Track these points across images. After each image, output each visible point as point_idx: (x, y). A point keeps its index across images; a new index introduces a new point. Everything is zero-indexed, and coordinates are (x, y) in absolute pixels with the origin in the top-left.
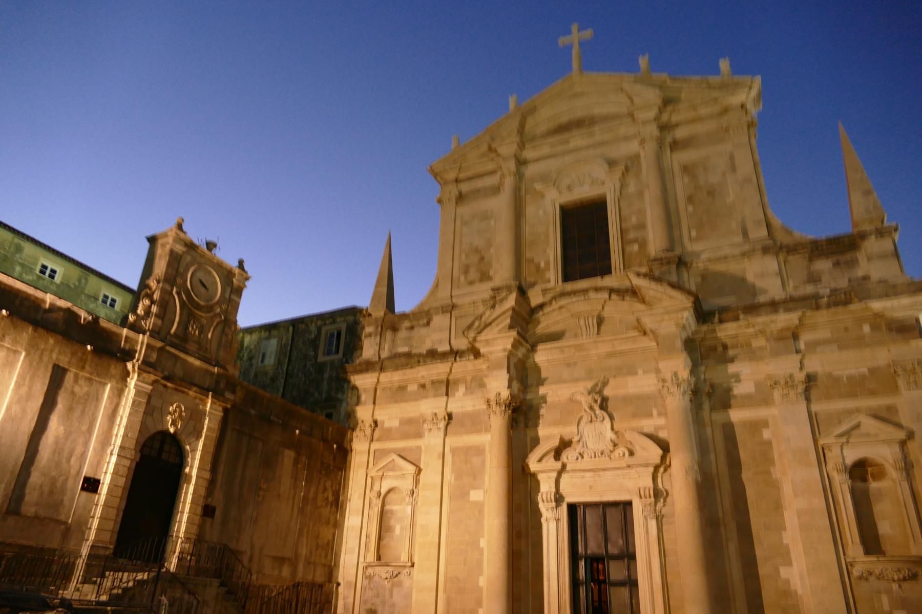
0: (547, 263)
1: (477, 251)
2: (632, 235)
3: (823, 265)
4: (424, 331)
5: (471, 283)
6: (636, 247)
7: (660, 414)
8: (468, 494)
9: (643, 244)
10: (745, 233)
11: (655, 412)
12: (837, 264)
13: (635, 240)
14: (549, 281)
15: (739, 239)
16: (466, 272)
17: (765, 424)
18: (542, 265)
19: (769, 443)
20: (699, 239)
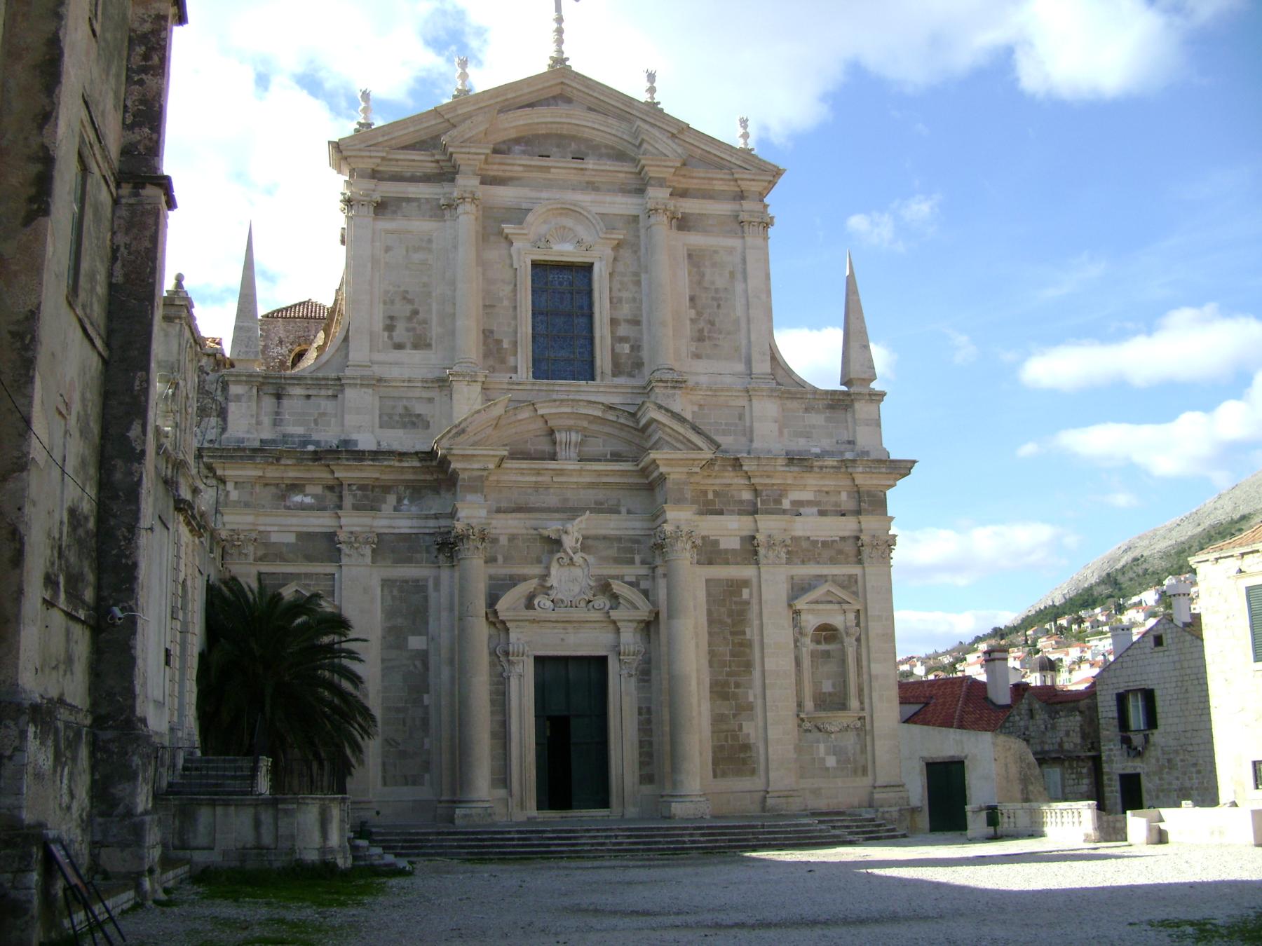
0: (515, 344)
1: (406, 299)
2: (623, 330)
3: (817, 419)
4: (327, 406)
5: (399, 346)
6: (626, 348)
7: (643, 562)
8: (406, 640)
9: (636, 348)
10: (749, 362)
11: (637, 558)
12: (828, 420)
13: (623, 340)
14: (515, 370)
15: (740, 367)
16: (390, 328)
17: (746, 583)
18: (505, 345)
19: (748, 603)
20: (697, 356)
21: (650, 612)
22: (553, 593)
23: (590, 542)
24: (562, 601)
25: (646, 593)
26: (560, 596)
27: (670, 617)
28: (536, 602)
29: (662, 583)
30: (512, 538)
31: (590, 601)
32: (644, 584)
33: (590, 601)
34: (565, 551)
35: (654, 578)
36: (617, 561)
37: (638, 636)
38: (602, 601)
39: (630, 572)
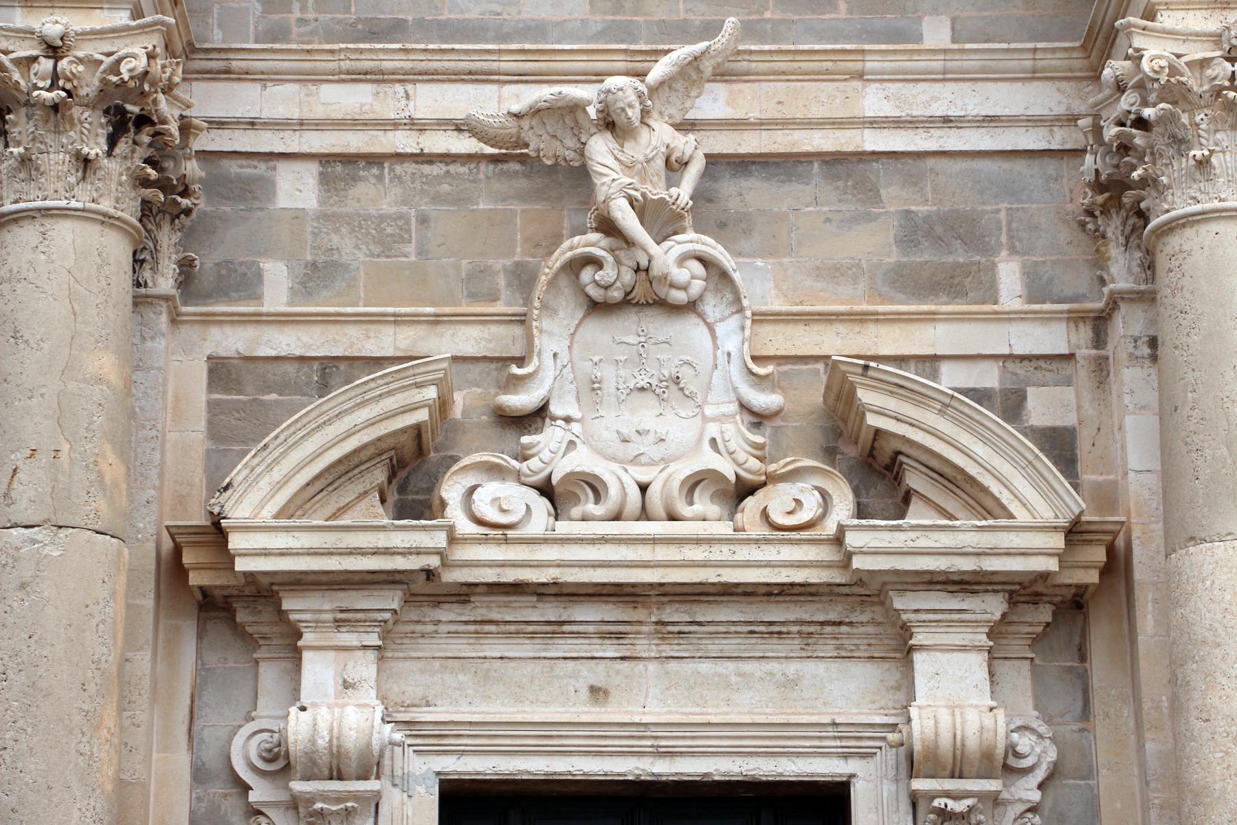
21: (1075, 532)
22: (550, 451)
23: (751, 194)
24: (596, 488)
25: (1060, 447)
26: (582, 461)
27: (1180, 534)
28: (451, 490)
29: (1132, 380)
30: (339, 167)
31: (743, 490)
32: (1046, 406)
33: (743, 490)
34: (608, 227)
35: (1101, 368)
36: (912, 282)
37: (1018, 677)
38: (814, 497)
39: (967, 340)
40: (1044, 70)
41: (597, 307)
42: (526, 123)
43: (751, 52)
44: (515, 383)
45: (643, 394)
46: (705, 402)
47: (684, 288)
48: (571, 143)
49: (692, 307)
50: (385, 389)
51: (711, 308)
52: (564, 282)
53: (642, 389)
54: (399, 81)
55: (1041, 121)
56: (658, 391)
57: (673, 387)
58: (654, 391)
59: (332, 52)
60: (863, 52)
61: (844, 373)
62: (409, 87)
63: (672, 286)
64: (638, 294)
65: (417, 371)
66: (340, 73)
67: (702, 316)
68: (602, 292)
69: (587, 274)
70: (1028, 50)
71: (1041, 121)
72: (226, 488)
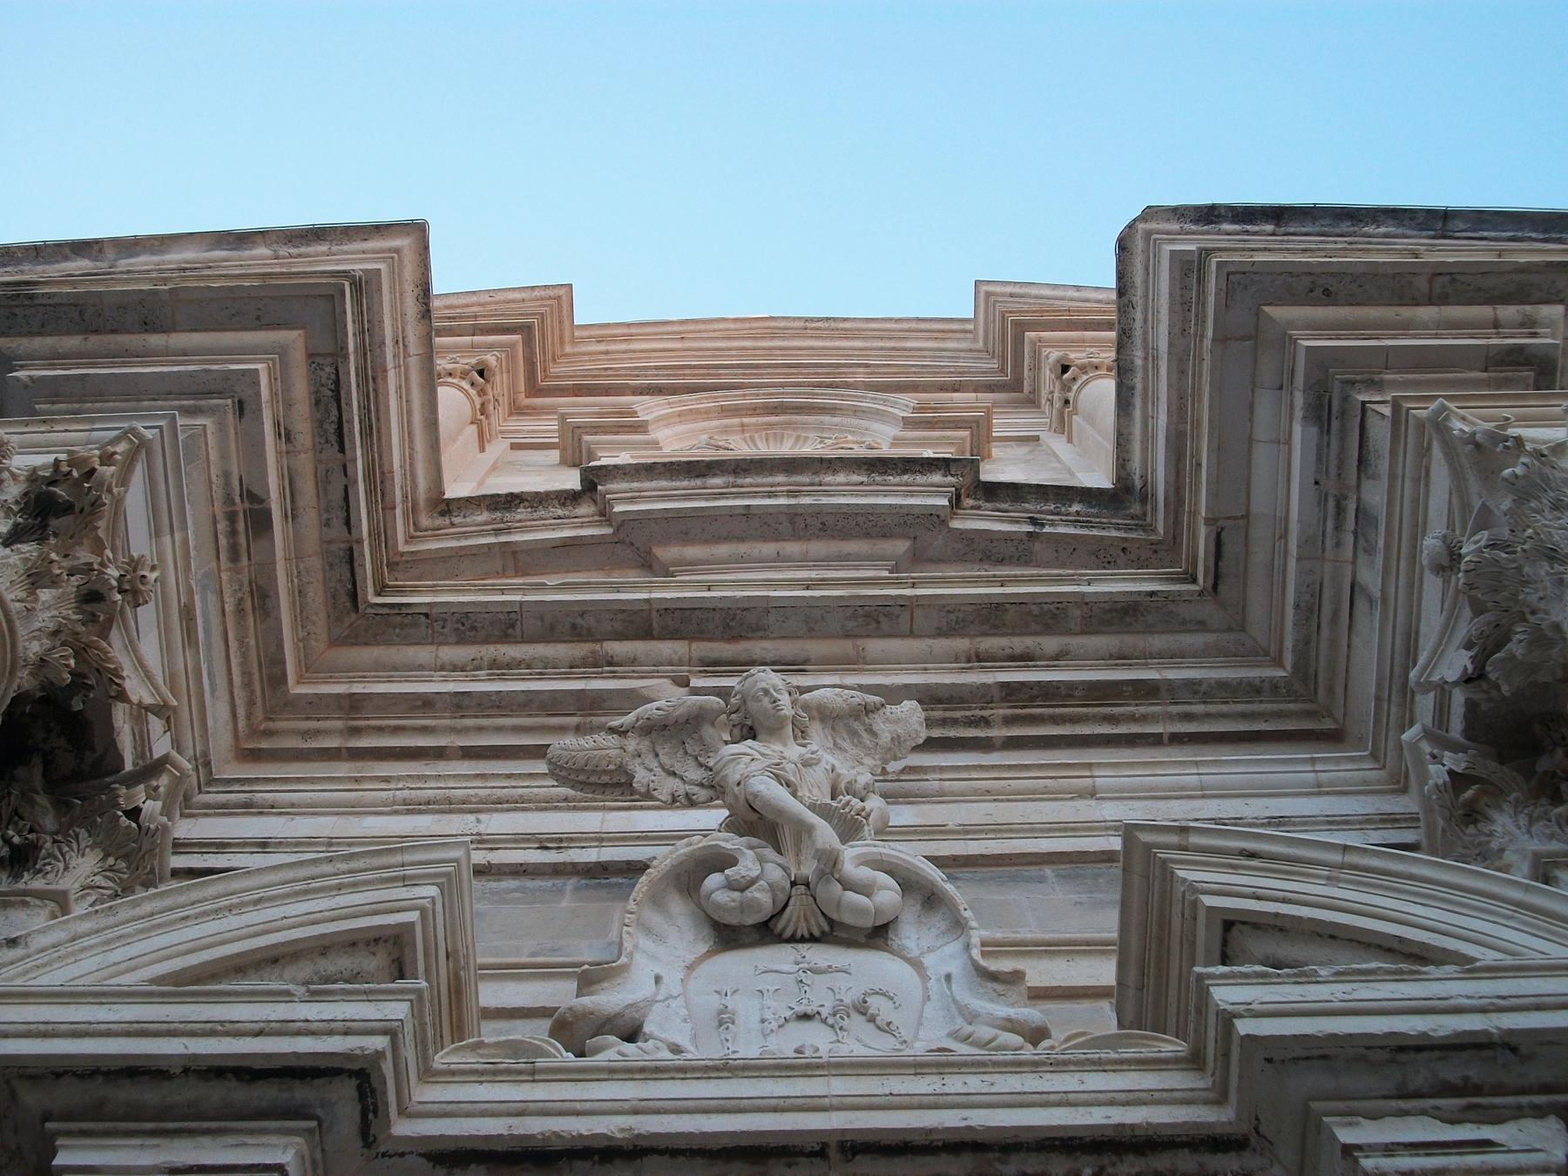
40: (1331, 783)
41: (728, 935)
42: (632, 743)
43: (942, 769)
44: (589, 979)
45: (807, 1025)
46: (916, 1038)
47: (866, 889)
48: (696, 774)
49: (878, 935)
50: (347, 879)
51: (913, 935)
52: (678, 905)
53: (805, 1017)
54: (471, 812)
55: (1347, 822)
56: (830, 1021)
57: (858, 1019)
58: (824, 1021)
59: (386, 779)
60: (1090, 766)
61: (1148, 847)
62: (482, 817)
63: (847, 885)
64: (793, 919)
65: (408, 858)
66: (394, 803)
67: (899, 954)
68: (736, 895)
69: (714, 880)
70: (1304, 761)
71: (1347, 822)
72: (12, 942)
